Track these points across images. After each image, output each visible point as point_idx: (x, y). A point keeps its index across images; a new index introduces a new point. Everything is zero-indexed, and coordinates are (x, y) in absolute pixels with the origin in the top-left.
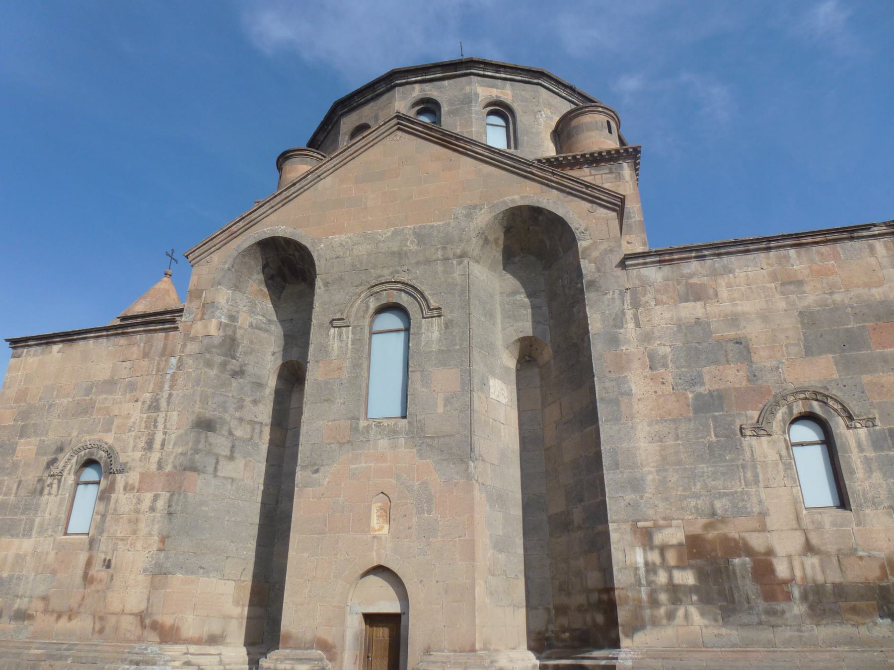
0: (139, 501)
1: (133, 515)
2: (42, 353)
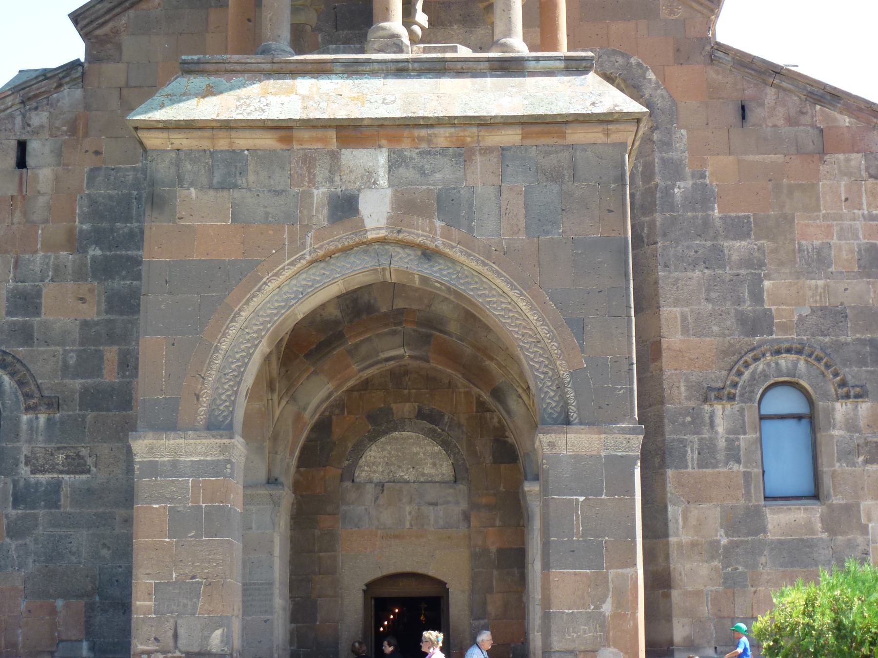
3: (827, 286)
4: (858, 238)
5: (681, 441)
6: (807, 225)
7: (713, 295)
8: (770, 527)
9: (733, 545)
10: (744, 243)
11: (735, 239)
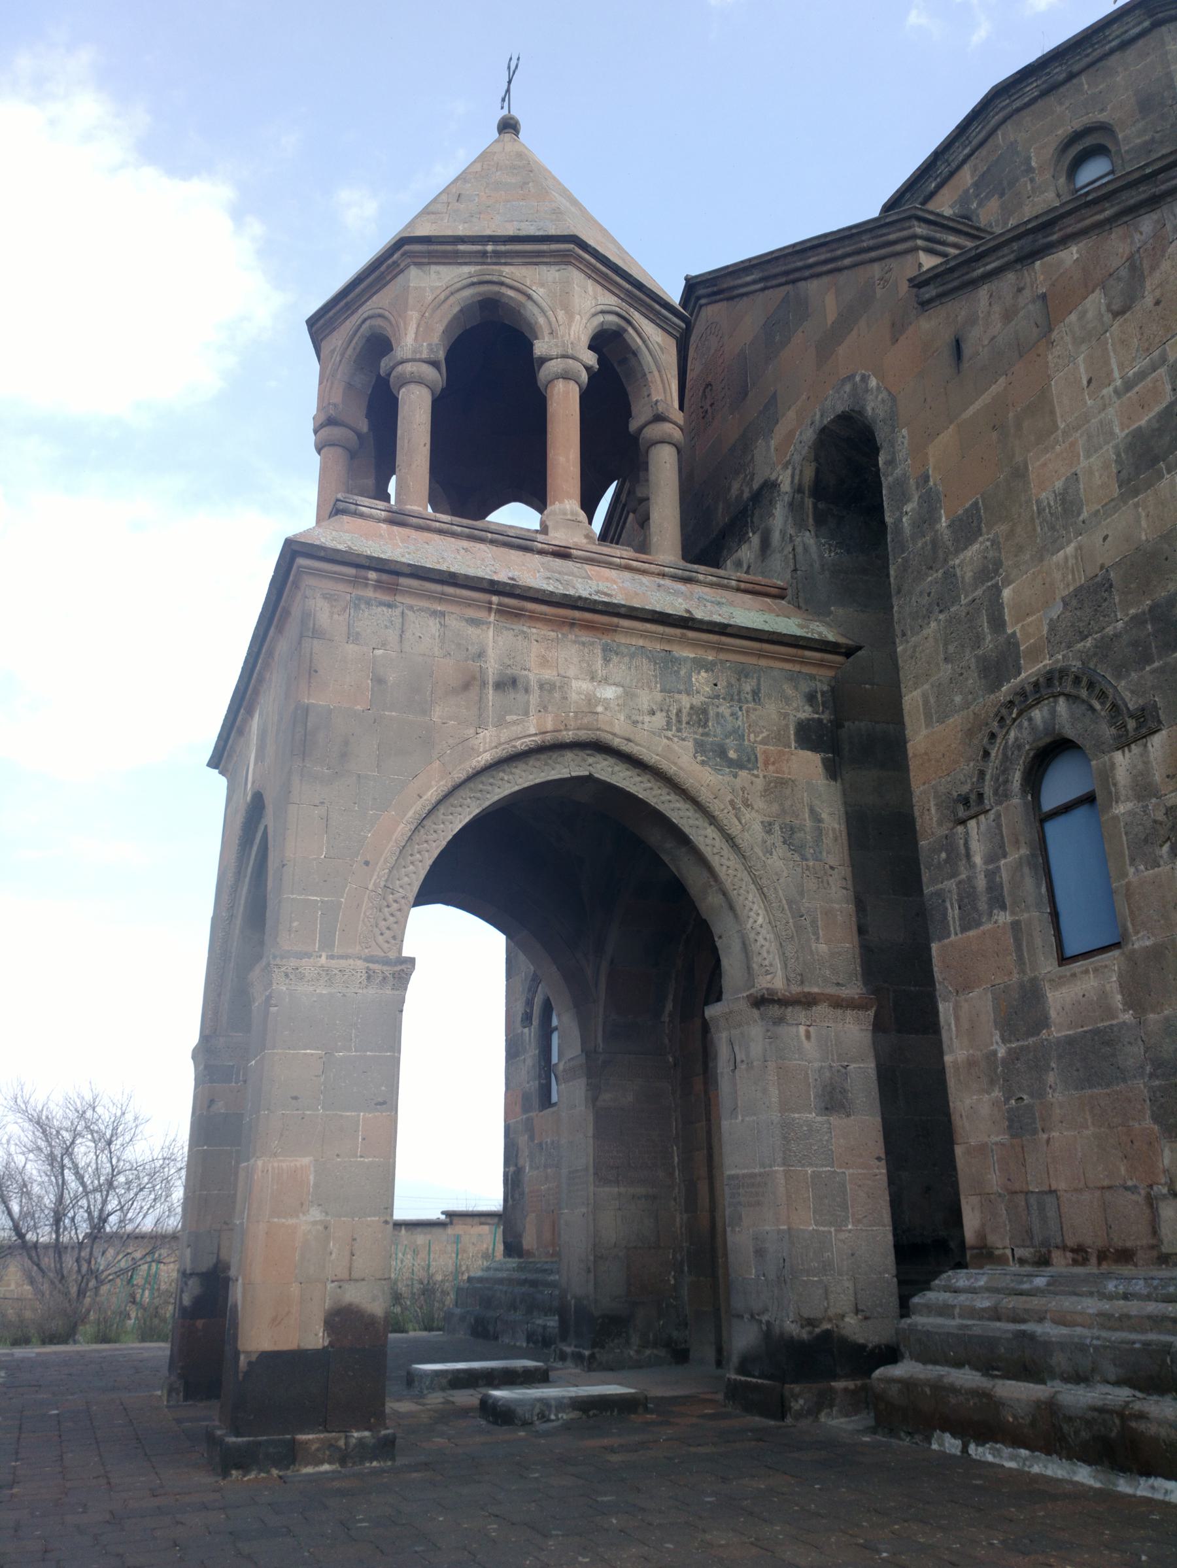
3: (1079, 548)
4: (1112, 433)
5: (939, 894)
6: (1044, 465)
7: (951, 649)
8: (1053, 1014)
9: (1014, 1056)
10: (976, 546)
11: (966, 548)
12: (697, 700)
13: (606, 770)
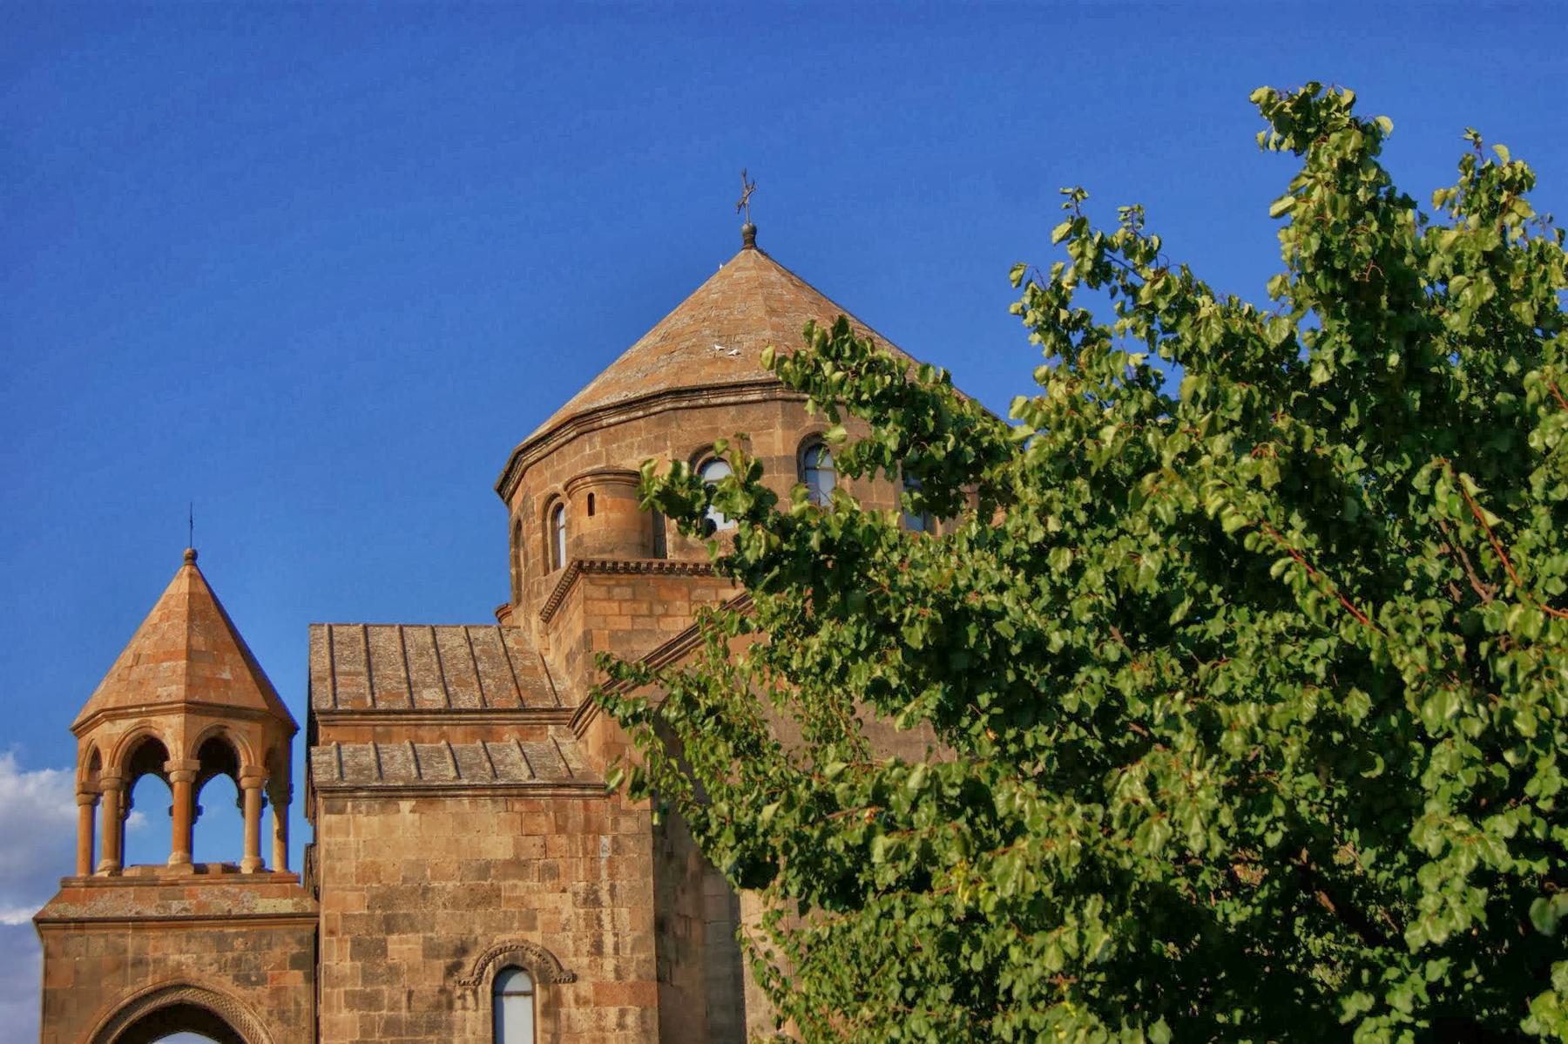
0: (600, 1017)
1: (598, 1034)
2: (383, 810)
12: (236, 954)
13: (188, 996)
